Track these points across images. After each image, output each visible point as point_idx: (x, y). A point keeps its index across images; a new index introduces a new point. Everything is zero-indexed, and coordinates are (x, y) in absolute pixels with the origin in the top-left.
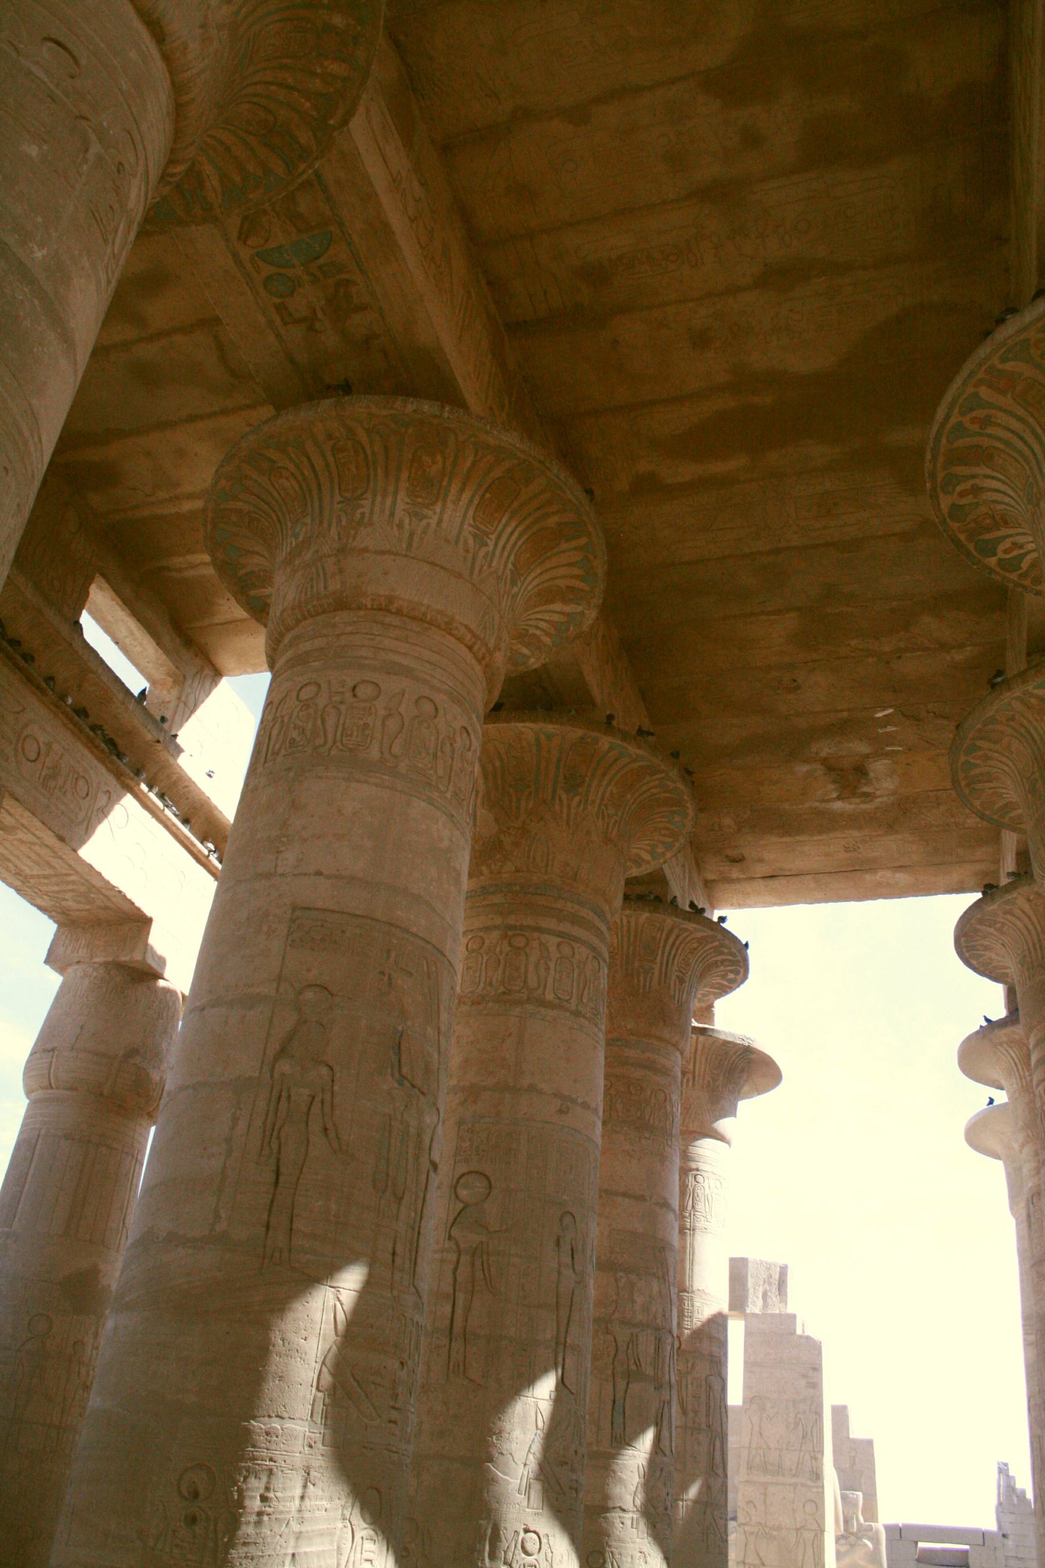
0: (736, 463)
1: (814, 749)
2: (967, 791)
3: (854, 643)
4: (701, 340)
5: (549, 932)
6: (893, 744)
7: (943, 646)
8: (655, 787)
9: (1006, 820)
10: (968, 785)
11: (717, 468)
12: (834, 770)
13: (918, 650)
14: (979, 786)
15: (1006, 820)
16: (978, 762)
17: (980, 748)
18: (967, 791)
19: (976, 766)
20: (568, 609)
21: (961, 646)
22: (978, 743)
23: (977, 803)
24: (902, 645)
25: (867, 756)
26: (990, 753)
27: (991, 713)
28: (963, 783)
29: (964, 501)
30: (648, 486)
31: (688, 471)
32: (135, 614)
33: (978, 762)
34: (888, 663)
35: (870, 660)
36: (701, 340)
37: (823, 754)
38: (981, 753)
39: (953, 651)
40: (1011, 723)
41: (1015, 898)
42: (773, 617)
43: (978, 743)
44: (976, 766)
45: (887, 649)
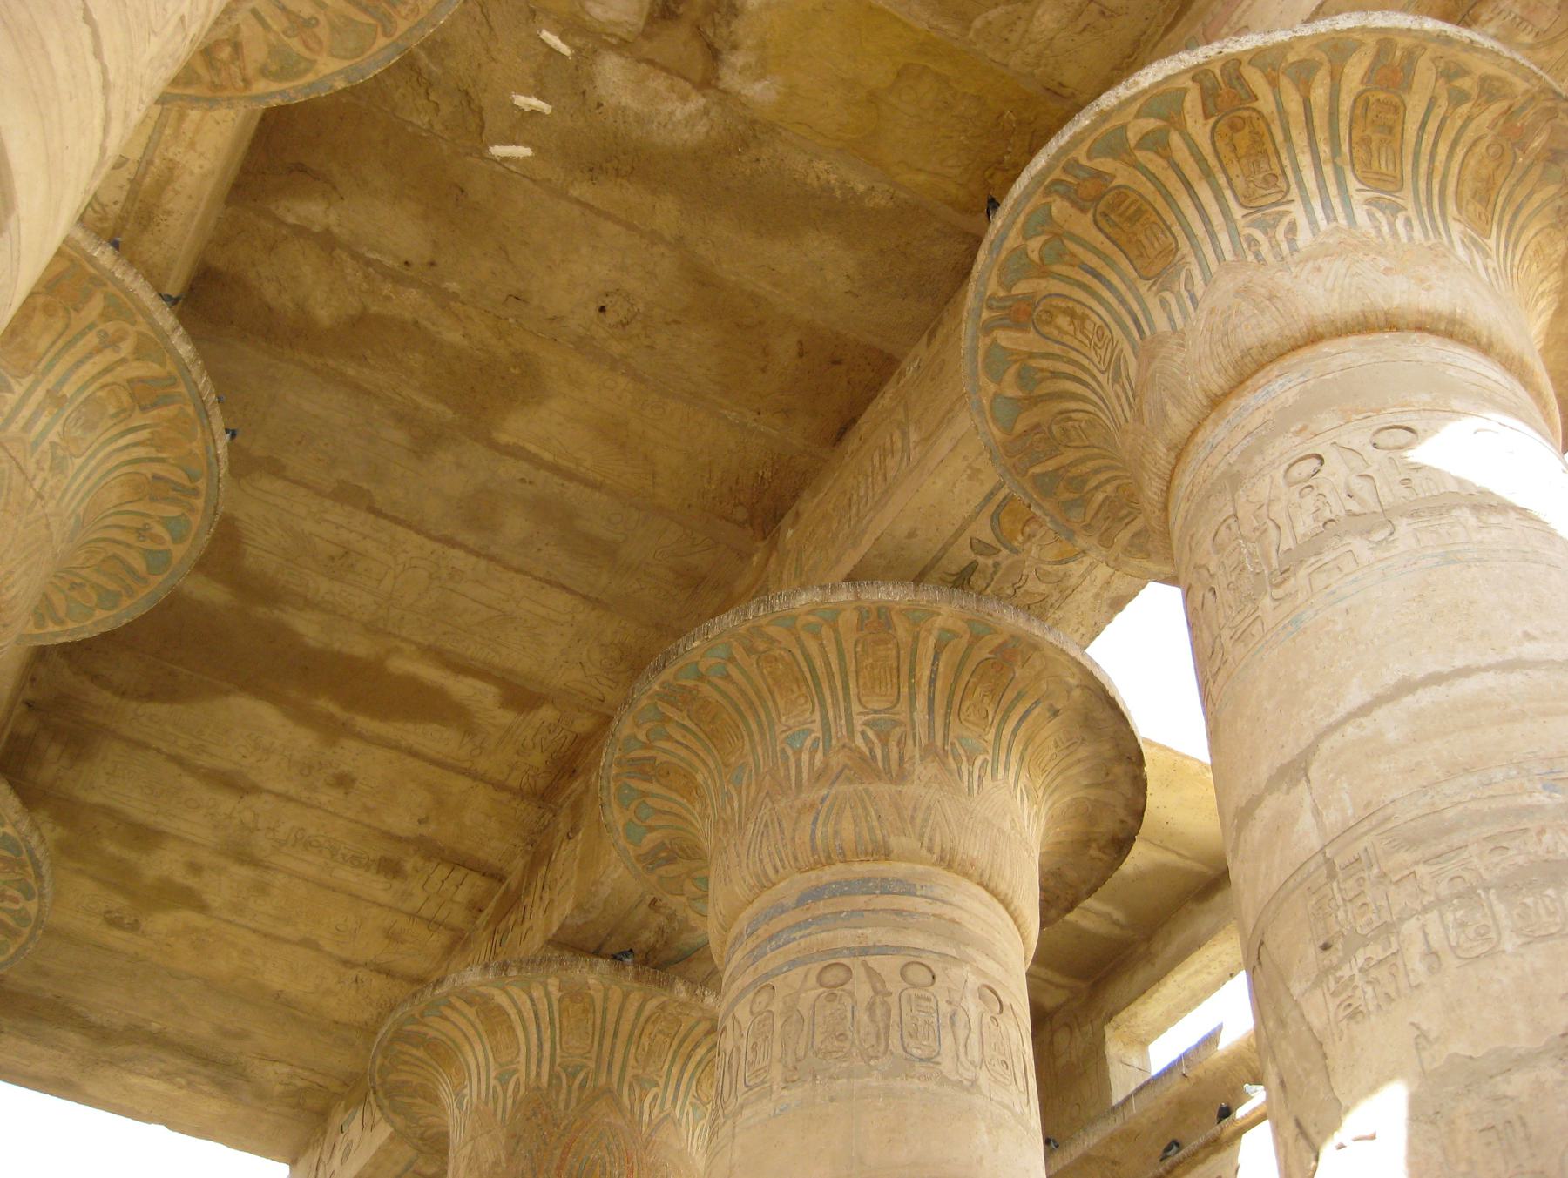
0: (401, 665)
1: (701, 128)
2: (202, 484)
3: (453, 336)
4: (343, 781)
5: (883, 950)
6: (552, 51)
7: (327, 242)
8: (669, 738)
9: (170, 367)
10: (195, 492)
11: (430, 673)
12: (710, 46)
13: (369, 263)
14: (179, 476)
15: (170, 367)
16: (159, 530)
17: (147, 553)
18: (202, 484)
19: (164, 522)
20: (496, 992)
21: (301, 231)
22: (139, 565)
23: (196, 446)
24: (387, 288)
25: (622, 46)
26: (131, 539)
27: (100, 614)
28: (199, 503)
29: (17, 894)
30: (521, 696)
31: (463, 688)
32: (1158, 979)
33: (159, 530)
34: (432, 264)
35: (453, 286)
36: (343, 781)
37: (697, 102)
38: (148, 545)
39: (317, 229)
40: (78, 581)
41: (264, 72)
42: (532, 448)
43: (139, 565)
44: (164, 522)
45: (413, 295)
